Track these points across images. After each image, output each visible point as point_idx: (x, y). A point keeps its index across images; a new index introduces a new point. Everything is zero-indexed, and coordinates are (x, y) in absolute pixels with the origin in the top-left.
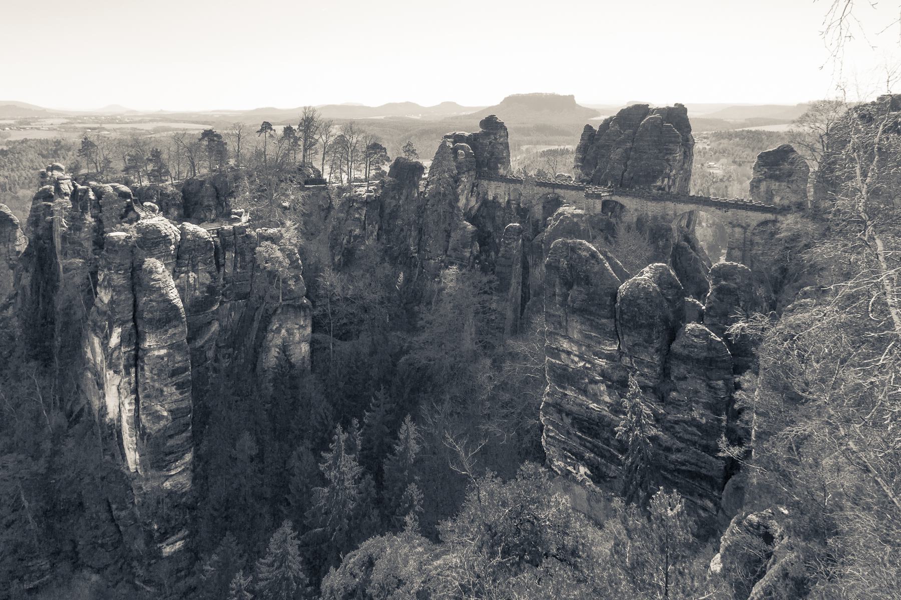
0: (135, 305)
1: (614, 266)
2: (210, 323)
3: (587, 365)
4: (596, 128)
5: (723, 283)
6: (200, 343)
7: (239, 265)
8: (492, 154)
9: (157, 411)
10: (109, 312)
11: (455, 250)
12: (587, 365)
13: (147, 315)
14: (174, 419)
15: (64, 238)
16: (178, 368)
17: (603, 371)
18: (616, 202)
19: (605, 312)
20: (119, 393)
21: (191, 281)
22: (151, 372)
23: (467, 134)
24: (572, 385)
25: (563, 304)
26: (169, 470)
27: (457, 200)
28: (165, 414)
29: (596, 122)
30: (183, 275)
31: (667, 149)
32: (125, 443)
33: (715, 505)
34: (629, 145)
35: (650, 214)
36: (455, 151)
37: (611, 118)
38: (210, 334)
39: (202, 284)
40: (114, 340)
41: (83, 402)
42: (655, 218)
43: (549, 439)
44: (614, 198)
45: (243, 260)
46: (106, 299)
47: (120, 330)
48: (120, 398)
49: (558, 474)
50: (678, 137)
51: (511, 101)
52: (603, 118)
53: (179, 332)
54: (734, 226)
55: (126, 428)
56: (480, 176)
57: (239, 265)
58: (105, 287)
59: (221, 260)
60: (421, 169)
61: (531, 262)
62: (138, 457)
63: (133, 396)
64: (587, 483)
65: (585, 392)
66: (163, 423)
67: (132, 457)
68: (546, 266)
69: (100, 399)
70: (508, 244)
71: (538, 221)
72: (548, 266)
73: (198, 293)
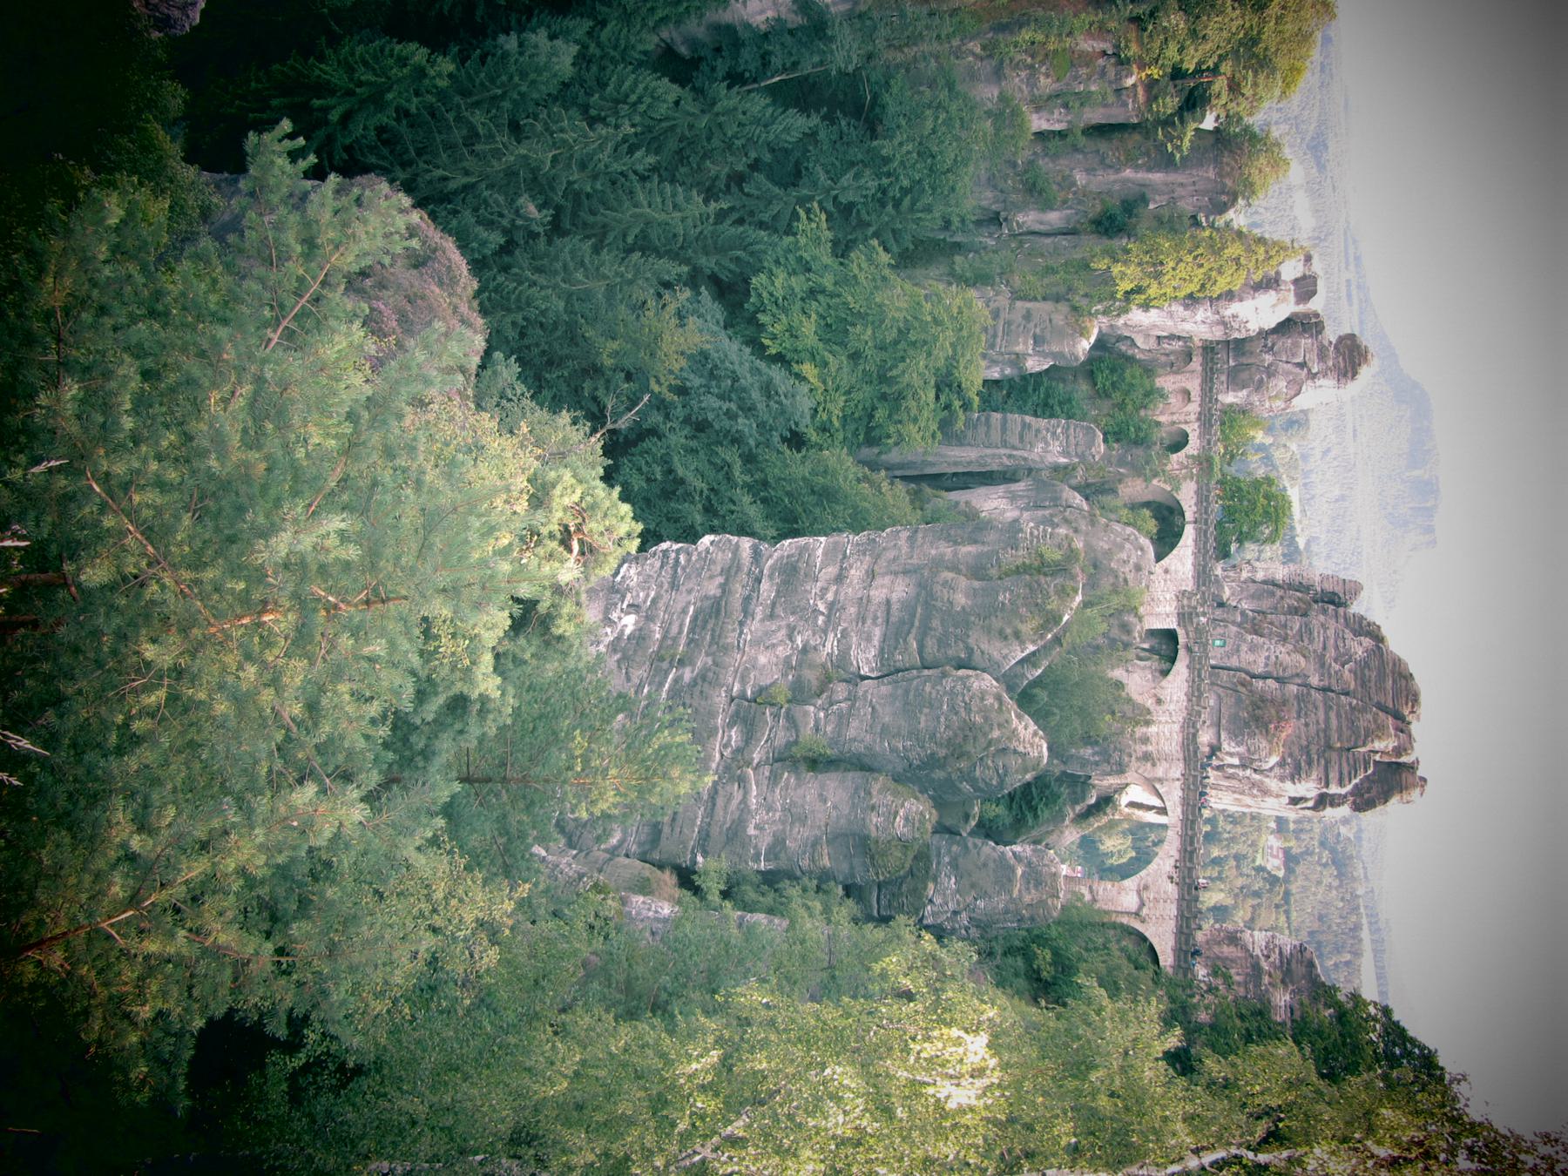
3: (821, 619)
4: (1356, 608)
5: (1019, 872)
8: (1271, 372)
11: (1028, 316)
12: (821, 619)
17: (815, 648)
18: (1173, 660)
24: (778, 592)
25: (938, 564)
27: (1146, 306)
31: (1309, 763)
33: (616, 848)
34: (1314, 680)
35: (1153, 729)
37: (1378, 638)
42: (1145, 740)
43: (673, 555)
44: (1182, 653)
50: (1341, 784)
54: (1139, 892)
56: (1209, 349)
60: (1222, 208)
61: (1019, 487)
64: (609, 630)
65: (772, 616)
68: (1016, 521)
70: (1054, 433)
71: (1114, 491)
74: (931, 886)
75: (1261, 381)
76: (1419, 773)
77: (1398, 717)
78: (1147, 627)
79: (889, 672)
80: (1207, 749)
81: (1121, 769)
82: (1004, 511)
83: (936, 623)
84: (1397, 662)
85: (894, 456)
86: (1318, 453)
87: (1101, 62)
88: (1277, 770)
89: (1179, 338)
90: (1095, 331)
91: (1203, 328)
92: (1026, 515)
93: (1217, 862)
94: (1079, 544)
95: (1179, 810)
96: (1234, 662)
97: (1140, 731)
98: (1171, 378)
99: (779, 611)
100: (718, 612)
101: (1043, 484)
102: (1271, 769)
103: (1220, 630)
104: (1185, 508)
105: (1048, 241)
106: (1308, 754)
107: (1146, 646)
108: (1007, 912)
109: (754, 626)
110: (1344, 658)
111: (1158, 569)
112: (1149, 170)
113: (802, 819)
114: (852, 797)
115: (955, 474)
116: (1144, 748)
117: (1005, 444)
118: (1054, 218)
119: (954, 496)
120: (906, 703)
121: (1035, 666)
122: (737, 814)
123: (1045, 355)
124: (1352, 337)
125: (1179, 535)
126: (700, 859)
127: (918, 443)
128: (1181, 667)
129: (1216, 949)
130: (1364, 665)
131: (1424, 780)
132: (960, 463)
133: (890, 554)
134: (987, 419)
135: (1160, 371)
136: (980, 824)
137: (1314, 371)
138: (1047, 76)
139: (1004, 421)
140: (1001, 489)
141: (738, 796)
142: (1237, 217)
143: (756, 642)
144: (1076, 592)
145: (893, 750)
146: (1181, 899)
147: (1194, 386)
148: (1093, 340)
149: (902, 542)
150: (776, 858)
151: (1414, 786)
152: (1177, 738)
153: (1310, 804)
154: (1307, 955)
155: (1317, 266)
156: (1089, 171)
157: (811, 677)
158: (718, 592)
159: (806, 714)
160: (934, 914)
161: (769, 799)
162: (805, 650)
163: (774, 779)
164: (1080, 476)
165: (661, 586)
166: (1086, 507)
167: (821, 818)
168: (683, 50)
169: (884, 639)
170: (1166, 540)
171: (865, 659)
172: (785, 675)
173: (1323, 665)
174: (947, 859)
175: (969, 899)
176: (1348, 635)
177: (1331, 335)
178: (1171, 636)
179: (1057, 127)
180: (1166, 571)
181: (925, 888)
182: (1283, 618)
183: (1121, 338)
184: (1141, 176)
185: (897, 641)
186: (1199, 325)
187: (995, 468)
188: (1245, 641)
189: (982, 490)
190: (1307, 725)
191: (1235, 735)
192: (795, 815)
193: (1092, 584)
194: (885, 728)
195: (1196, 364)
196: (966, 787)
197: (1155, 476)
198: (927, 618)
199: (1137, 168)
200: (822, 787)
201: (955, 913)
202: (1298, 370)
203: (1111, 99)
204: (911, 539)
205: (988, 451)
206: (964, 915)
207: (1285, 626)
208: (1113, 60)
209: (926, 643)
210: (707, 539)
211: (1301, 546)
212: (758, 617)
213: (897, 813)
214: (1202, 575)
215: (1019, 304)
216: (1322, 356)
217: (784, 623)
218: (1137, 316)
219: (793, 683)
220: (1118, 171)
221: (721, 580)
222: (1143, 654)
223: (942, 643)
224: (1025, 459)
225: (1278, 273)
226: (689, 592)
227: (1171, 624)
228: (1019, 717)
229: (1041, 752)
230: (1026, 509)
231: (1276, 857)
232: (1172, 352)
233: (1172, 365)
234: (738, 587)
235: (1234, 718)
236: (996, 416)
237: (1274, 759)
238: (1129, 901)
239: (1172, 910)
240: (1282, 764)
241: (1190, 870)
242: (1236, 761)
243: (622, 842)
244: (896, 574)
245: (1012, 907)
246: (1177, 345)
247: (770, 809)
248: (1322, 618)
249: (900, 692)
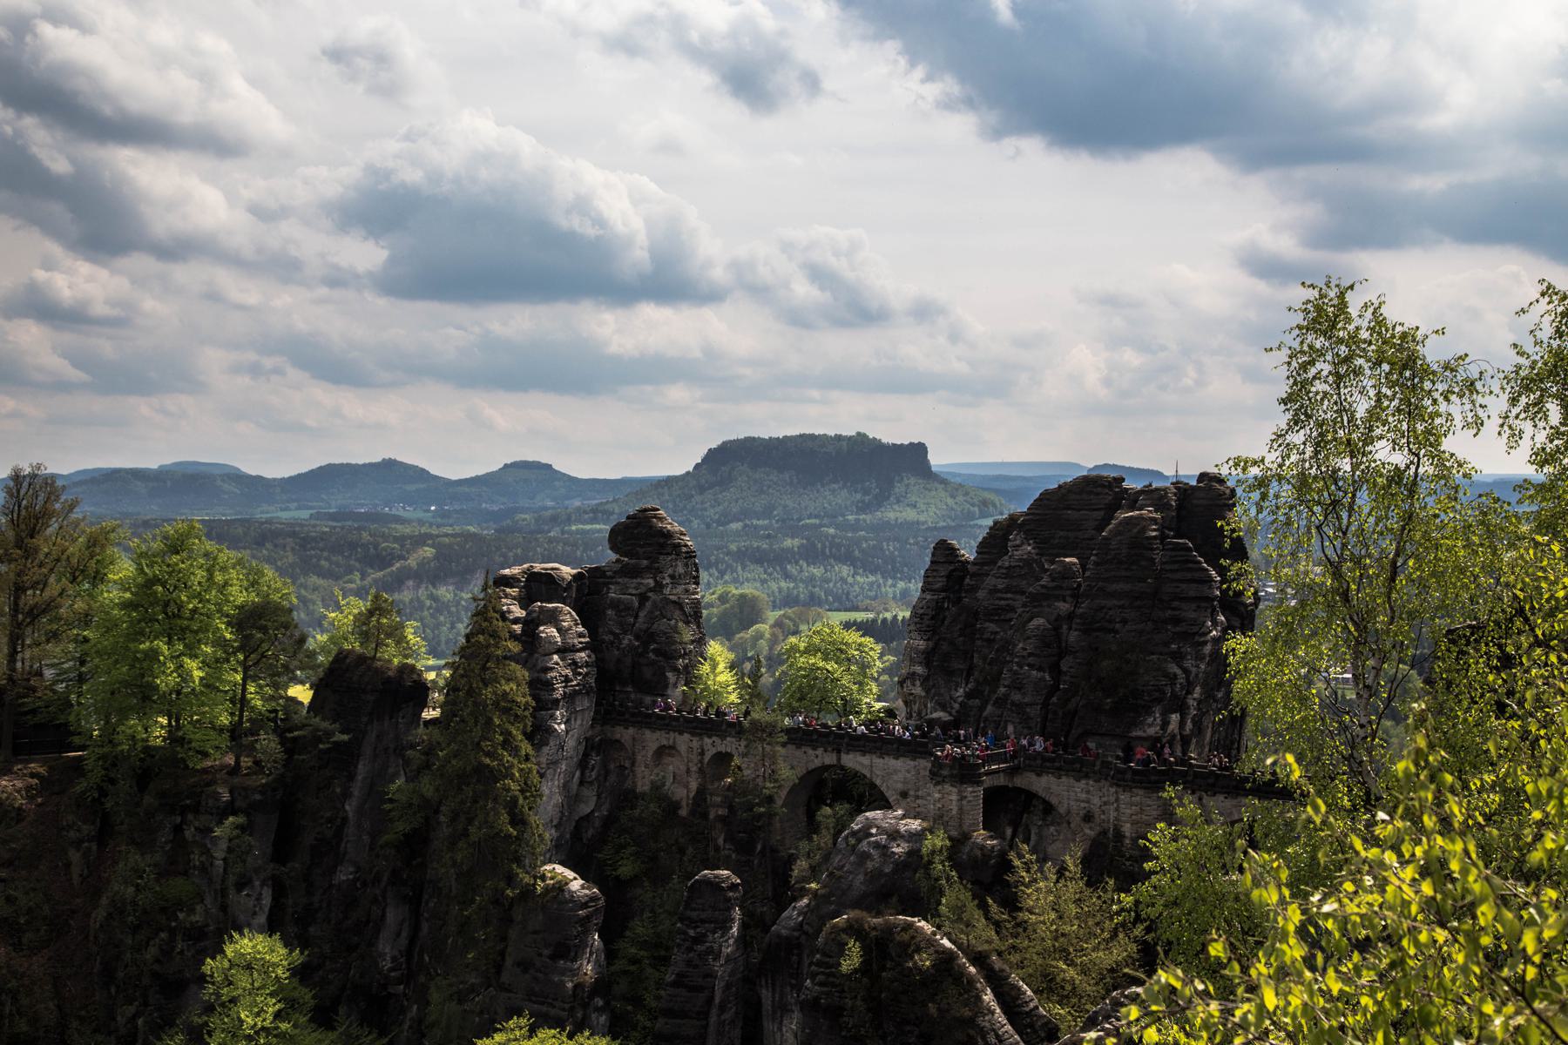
4: (968, 552)
11: (524, 965)
18: (1030, 796)
23: (567, 571)
31: (1177, 621)
34: (1064, 607)
36: (531, 624)
44: (1020, 781)
61: (766, 995)
75: (657, 652)
76: (1194, 483)
87: (189, 833)
88: (1188, 664)
89: (586, 755)
90: (559, 869)
98: (640, 770)
102: (1186, 671)
104: (817, 763)
105: (425, 927)
107: (1009, 832)
117: (706, 1015)
118: (393, 915)
124: (614, 532)
125: (856, 776)
135: (628, 784)
137: (651, 582)
138: (192, 911)
140: (769, 1026)
142: (433, 670)
144: (911, 925)
147: (653, 739)
148: (570, 874)
151: (1210, 489)
176: (1005, 562)
177: (607, 557)
179: (267, 901)
180: (904, 795)
182: (979, 643)
187: (737, 1033)
188: (1006, 696)
190: (1124, 622)
195: (625, 734)
199: (346, 795)
202: (648, 604)
207: (989, 641)
208: (190, 817)
215: (505, 978)
220: (345, 820)
224: (728, 986)
225: (516, 621)
227: (974, 794)
230: (799, 987)
232: (605, 766)
233: (623, 768)
240: (1178, 657)
242: (1175, 717)
248: (981, 594)
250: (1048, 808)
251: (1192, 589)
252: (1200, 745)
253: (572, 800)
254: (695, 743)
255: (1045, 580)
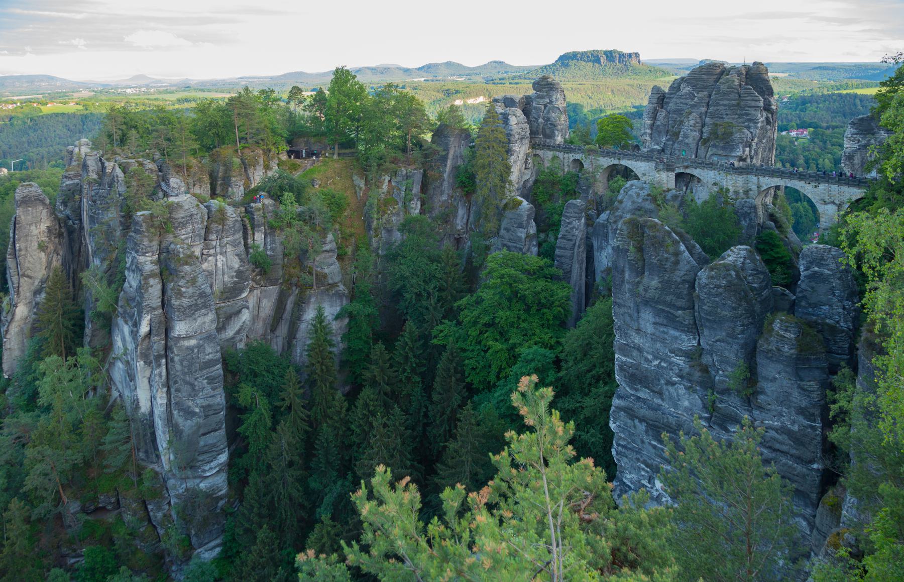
0: (164, 291)
1: (690, 249)
2: (239, 312)
3: (663, 364)
5: (816, 269)
6: (230, 332)
7: (269, 248)
8: (547, 120)
9: (189, 407)
10: (138, 298)
11: (507, 230)
12: (663, 364)
13: (175, 302)
14: (206, 416)
15: (92, 219)
16: (210, 361)
18: (693, 176)
19: (680, 303)
20: (151, 386)
21: (220, 264)
22: (182, 364)
24: (646, 387)
25: (634, 294)
26: (204, 471)
28: (197, 410)
29: (665, 83)
30: (210, 258)
31: (748, 115)
32: (158, 440)
33: (809, 523)
34: (704, 109)
35: (731, 188)
37: (682, 79)
38: (241, 324)
39: (231, 268)
40: (144, 329)
41: (115, 394)
42: (737, 193)
43: (620, 448)
44: (688, 171)
45: (273, 242)
46: (134, 284)
47: (149, 317)
48: (151, 391)
49: (630, 488)
51: (566, 60)
52: (672, 79)
53: (207, 320)
54: (825, 203)
55: (159, 424)
56: (533, 146)
57: (269, 248)
58: (133, 271)
59: (250, 241)
61: (595, 244)
62: (172, 457)
63: (165, 390)
64: (664, 499)
65: (660, 394)
66: (195, 420)
67: (167, 458)
68: (613, 248)
69: (131, 391)
71: (601, 197)
72: (616, 249)
73: (226, 278)
74: (827, 321)
77: (722, 73)
78: (674, 187)
79: (695, 329)
80: (741, 163)
81: (755, 207)
82: (608, 254)
83: (668, 299)
84: (694, 72)
85: (573, 306)
86: (590, 101)
87: (393, 184)
88: (752, 130)
91: (523, 148)
92: (610, 242)
93: (807, 162)
94: (628, 216)
95: (776, 179)
96: (693, 147)
97: (731, 194)
99: (657, 389)
100: (655, 426)
101: (595, 233)
103: (677, 152)
106: (743, 115)
107: (684, 188)
108: (841, 278)
109: (665, 405)
110: (691, 96)
111: (643, 179)
112: (446, 166)
113: (788, 395)
114: (773, 361)
115: (586, 277)
116: (741, 194)
117: (572, 249)
118: (461, 212)
119: (598, 278)
120: (715, 321)
121: (694, 247)
122: (785, 437)
123: (528, 223)
126: (815, 466)
127: (566, 293)
128: (696, 172)
129: (857, 167)
130: (694, 87)
131: (755, 63)
132: (581, 273)
133: (628, 318)
134: (559, 256)
136: (786, 286)
139: (560, 248)
141: (772, 433)
143: (676, 406)
145: (742, 332)
146: (827, 182)
149: (622, 311)
150: (813, 415)
152: (735, 177)
153: (770, 116)
154: (856, 121)
155: (500, 96)
156: (442, 193)
157: (697, 375)
158: (644, 424)
159: (720, 381)
160: (846, 322)
161: (774, 413)
162: (681, 376)
163: (760, 408)
164: (593, 212)
165: (638, 460)
166: (608, 212)
167: (785, 382)
168: (347, 388)
169: (675, 328)
170: (628, 174)
171: (688, 342)
172: (695, 391)
173: (695, 106)
174: (810, 310)
175: (835, 300)
176: (679, 93)
177: (531, 92)
178: (679, 176)
179: (419, 206)
180: (644, 175)
181: (828, 325)
183: (524, 186)
184: (448, 169)
185: (678, 322)
186: (521, 150)
189: (596, 264)
191: (733, 149)
192: (784, 400)
193: (649, 212)
194: (728, 335)
195: (538, 152)
196: (765, 293)
197: (595, 176)
198: (664, 303)
200: (766, 379)
201: (844, 308)
203: (410, 181)
204: (620, 306)
205: (575, 257)
206: (845, 304)
209: (681, 306)
210: (612, 426)
211: (635, 110)
212: (660, 402)
213: (781, 336)
214: (647, 158)
216: (542, 97)
217: (665, 387)
218: (514, 176)
219: (701, 387)
221: (636, 421)
222: (689, 191)
223: (679, 296)
225: (501, 114)
226: (643, 442)
227: (672, 175)
228: (724, 259)
229: (743, 250)
230: (607, 241)
231: (802, 133)
234: (643, 411)
235: (724, 148)
236: (557, 252)
237: (746, 131)
238: (831, 209)
239: (834, 187)
240: (748, 128)
241: (810, 176)
242: (747, 149)
243: (805, 518)
244: (638, 317)
245: (838, 275)
246: (530, 160)
247: (781, 415)
249: (707, 324)
250: (699, 180)
251: (753, 103)
252: (757, 159)
253: (522, 174)
254: (566, 155)
255: (696, 99)
